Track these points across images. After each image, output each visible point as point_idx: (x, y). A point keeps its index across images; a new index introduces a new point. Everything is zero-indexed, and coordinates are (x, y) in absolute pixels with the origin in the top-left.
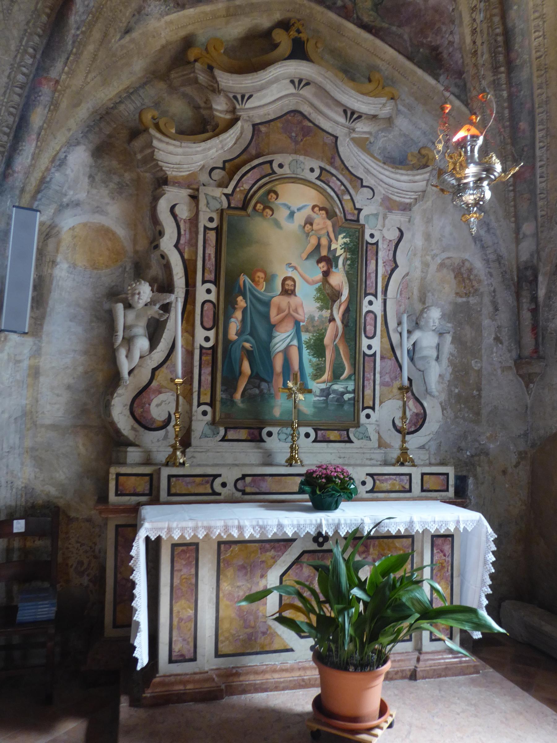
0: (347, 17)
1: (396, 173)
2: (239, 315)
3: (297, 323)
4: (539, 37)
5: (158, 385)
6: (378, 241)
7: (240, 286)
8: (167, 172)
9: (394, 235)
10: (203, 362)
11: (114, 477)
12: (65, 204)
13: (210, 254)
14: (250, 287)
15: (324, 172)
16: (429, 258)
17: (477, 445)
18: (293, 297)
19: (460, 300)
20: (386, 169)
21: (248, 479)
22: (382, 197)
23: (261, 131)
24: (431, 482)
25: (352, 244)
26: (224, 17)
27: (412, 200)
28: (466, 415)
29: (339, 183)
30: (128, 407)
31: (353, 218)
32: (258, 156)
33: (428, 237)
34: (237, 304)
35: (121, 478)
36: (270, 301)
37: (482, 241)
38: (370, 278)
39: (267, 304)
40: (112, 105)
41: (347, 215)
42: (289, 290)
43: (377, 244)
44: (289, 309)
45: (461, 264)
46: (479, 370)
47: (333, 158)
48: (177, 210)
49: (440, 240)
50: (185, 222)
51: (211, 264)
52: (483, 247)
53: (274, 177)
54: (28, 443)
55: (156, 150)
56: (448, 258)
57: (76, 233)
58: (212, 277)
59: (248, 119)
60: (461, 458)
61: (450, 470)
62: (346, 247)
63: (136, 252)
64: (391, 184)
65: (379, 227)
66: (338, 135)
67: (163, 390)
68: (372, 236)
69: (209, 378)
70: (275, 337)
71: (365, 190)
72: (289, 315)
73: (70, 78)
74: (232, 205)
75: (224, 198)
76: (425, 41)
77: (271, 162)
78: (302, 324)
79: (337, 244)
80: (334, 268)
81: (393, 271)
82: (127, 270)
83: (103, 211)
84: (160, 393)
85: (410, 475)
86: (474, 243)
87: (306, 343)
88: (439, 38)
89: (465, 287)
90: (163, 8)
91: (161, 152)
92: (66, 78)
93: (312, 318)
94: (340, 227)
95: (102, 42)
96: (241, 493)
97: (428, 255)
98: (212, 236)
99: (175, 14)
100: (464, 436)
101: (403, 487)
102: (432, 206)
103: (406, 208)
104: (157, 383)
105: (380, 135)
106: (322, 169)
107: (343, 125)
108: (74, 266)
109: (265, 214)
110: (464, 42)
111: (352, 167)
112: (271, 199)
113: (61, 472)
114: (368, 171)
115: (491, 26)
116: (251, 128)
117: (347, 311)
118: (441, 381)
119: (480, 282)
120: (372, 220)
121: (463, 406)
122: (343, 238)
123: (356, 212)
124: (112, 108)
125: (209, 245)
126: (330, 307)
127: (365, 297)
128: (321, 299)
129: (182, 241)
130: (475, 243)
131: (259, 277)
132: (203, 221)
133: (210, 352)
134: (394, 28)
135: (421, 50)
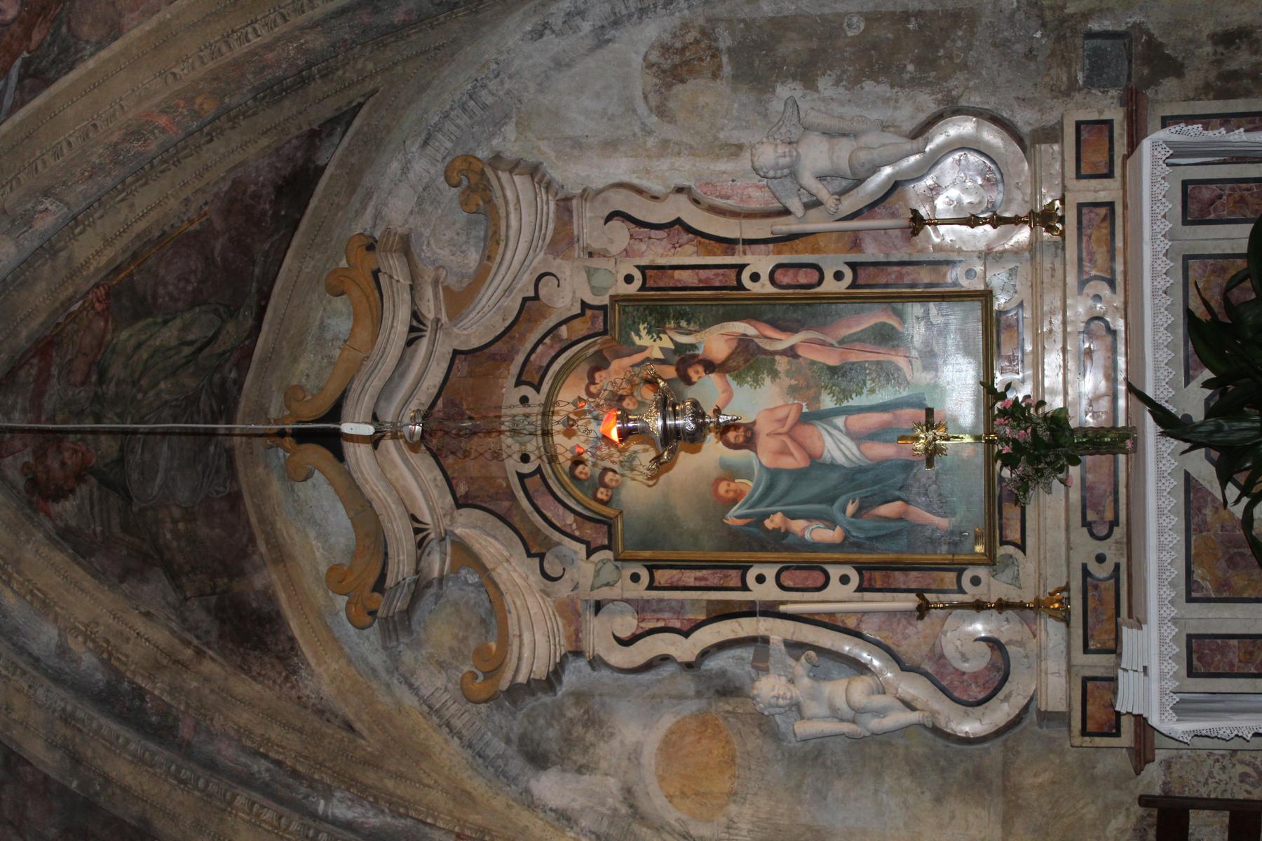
0: (250, 355)
1: (507, 237)
2: (797, 526)
3: (805, 419)
4: (255, 30)
5: (930, 659)
6: (638, 267)
7: (747, 525)
8: (563, 652)
9: (620, 231)
10: (885, 586)
11: (1087, 739)
12: (630, 811)
13: (696, 579)
14: (746, 506)
15: (523, 378)
16: (651, 142)
17: (1020, 16)
18: (757, 428)
19: (727, 69)
20: (502, 259)
21: (1091, 516)
22: (550, 257)
23: (467, 493)
25: (649, 319)
26: (285, 566)
27: (550, 198)
28: (959, 43)
29: (540, 348)
30: (970, 709)
31: (601, 318)
32: (512, 497)
33: (610, 146)
34: (780, 528)
35: (1091, 727)
36: (768, 469)
37: (603, 27)
38: (708, 279)
39: (774, 475)
40: (455, 738)
41: (596, 330)
42: (745, 436)
43: (642, 269)
44: (779, 434)
45: (655, 69)
46: (867, 19)
47: (493, 357)
48: (625, 634)
49: (611, 118)
50: (643, 620)
51: (713, 577)
52: (616, 23)
53: (547, 470)
55: (532, 676)
56: (646, 98)
57: (677, 793)
58: (735, 574)
59: (449, 517)
60: (1048, 52)
62: (657, 329)
63: (699, 694)
64: (526, 245)
65: (610, 265)
66: (451, 351)
67: (937, 650)
68: (629, 279)
69: (913, 574)
70: (832, 458)
71: (542, 292)
72: (789, 434)
73: (439, 813)
74: (606, 542)
75: (596, 557)
76: (270, 212)
77: (522, 477)
78: (805, 410)
79: (652, 346)
80: (697, 352)
81: (689, 229)
82: (730, 708)
83: (635, 751)
84: (942, 656)
85: (1080, 206)
86: (610, 44)
87: (839, 400)
88: (264, 192)
89: (701, 59)
90: (303, 673)
91: (534, 669)
92: (442, 819)
93: (793, 390)
94: (619, 342)
95: (377, 767)
96: (1115, 529)
97: (645, 143)
98: (662, 576)
99: (304, 649)
100: (1002, 46)
101: (1104, 220)
102: (548, 139)
103: (565, 205)
104: (926, 661)
105: (428, 254)
106: (519, 383)
107: (433, 342)
108: (732, 794)
109: (614, 484)
110: (269, 147)
111: (504, 320)
112: (586, 474)
113: (1084, 811)
114: (508, 290)
115: (244, 114)
116: (464, 511)
117: (776, 325)
118: (892, 103)
119: (685, 26)
120: (599, 280)
121: (941, 53)
122: (640, 337)
123: (589, 312)
124: (460, 738)
125: (680, 579)
126: (769, 357)
127: (745, 289)
128: (757, 374)
129: (677, 625)
130: (608, 41)
131: (727, 491)
132: (639, 591)
133: (866, 574)
134: (257, 271)
135: (283, 213)
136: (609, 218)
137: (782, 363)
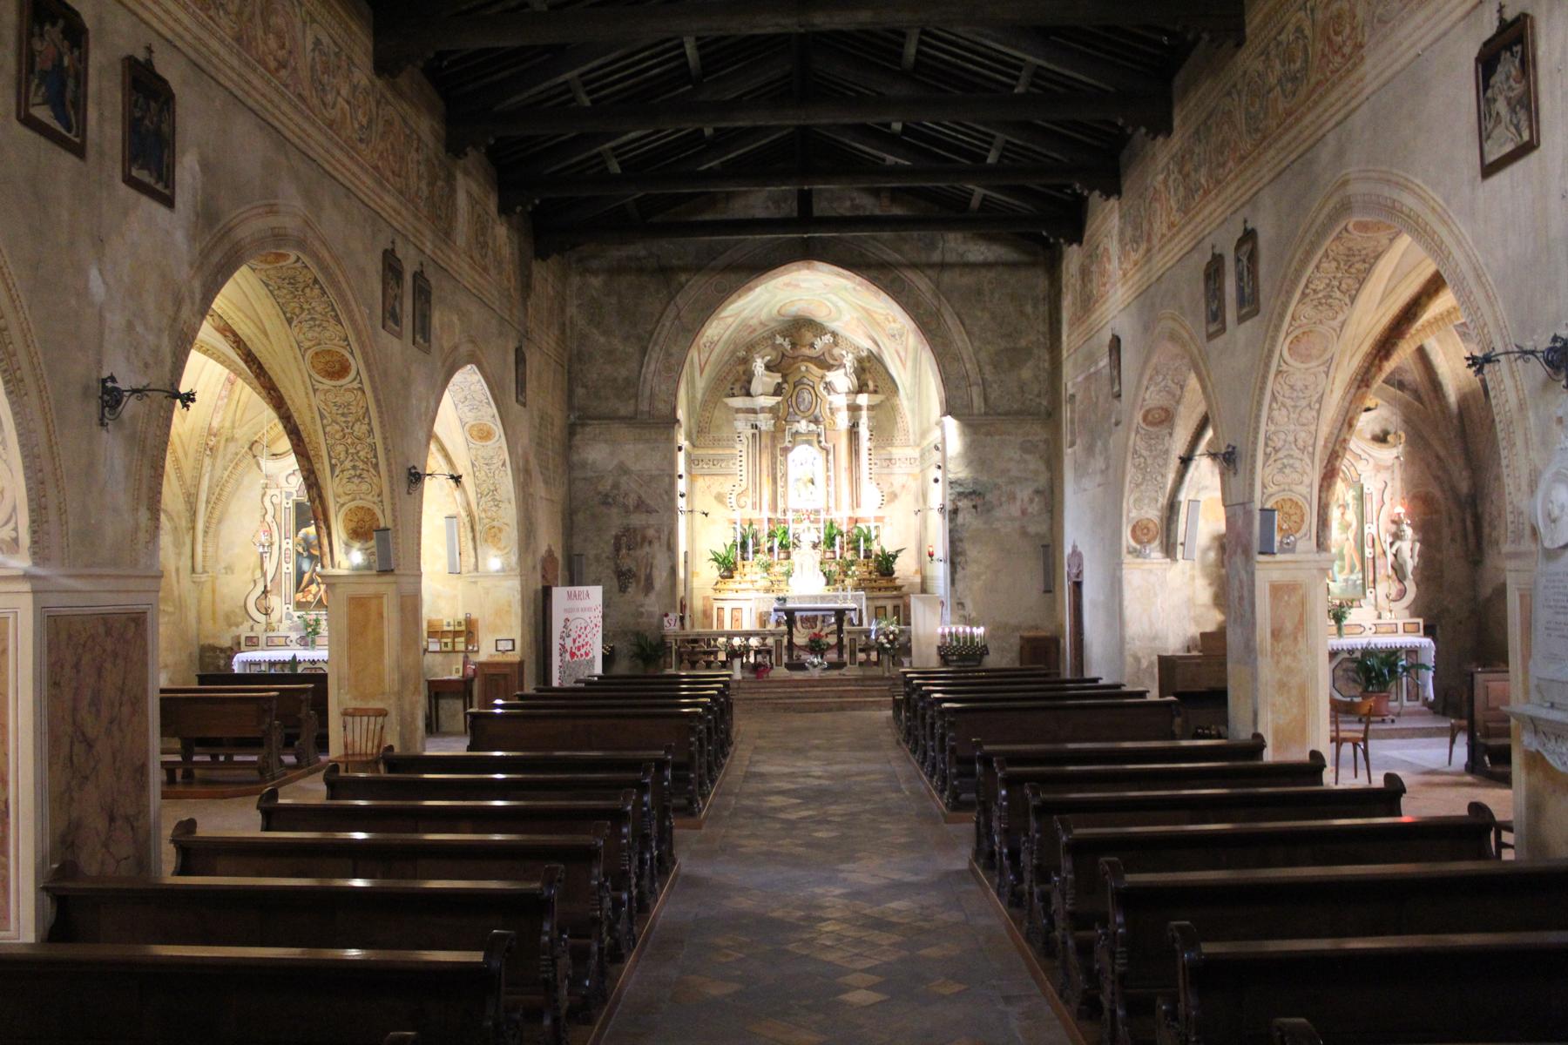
24: (1408, 628)
54: (1192, 614)
61: (1420, 621)
62: (1354, 498)
117: (1356, 533)
136: (1386, 483)
137: (1344, 536)
